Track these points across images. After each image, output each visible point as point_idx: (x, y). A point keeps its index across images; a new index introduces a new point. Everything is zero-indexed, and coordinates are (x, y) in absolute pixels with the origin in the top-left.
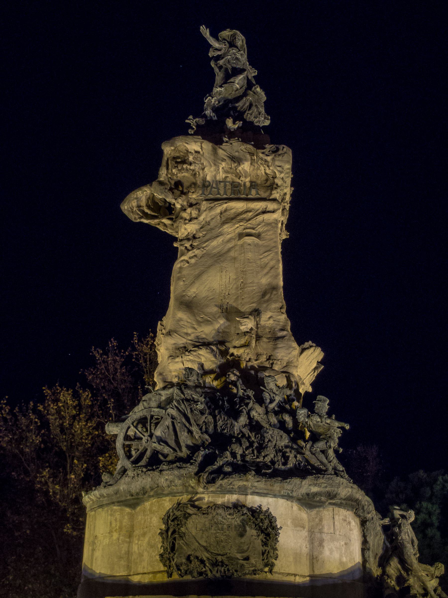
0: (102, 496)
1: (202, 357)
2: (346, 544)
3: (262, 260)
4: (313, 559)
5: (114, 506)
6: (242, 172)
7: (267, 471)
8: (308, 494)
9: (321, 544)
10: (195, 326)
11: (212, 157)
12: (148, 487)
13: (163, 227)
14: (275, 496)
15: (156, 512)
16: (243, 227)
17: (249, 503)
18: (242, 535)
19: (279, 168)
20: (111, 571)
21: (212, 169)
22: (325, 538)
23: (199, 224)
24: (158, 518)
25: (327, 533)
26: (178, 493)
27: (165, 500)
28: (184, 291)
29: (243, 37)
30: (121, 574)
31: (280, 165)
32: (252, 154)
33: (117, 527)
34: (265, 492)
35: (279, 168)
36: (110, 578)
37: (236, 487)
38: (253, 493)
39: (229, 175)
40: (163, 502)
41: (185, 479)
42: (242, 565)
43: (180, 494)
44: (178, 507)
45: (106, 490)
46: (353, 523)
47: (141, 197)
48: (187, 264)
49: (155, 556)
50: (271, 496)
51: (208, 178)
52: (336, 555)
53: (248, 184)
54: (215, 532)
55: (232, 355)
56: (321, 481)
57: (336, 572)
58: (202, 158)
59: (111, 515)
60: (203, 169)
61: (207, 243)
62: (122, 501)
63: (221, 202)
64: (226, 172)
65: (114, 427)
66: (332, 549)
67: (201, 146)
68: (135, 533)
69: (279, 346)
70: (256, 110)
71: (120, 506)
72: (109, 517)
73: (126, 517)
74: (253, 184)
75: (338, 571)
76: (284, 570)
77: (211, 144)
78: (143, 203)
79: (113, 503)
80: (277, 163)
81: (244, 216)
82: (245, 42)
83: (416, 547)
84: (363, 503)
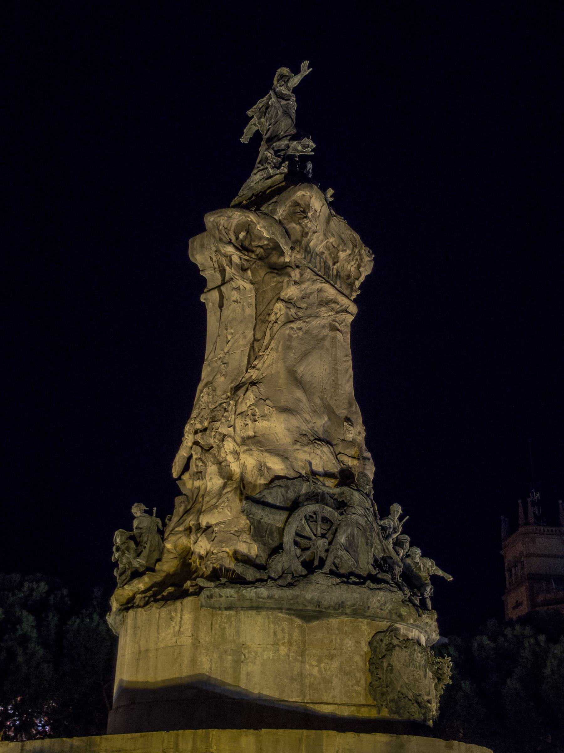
0: (270, 597)
5: (281, 612)
11: (325, 225)
12: (349, 603)
13: (228, 262)
15: (351, 633)
20: (280, 694)
23: (301, 291)
24: (353, 641)
26: (380, 618)
27: (362, 622)
28: (294, 365)
30: (294, 700)
32: (355, 246)
33: (286, 641)
36: (284, 703)
39: (326, 252)
40: (360, 624)
43: (380, 620)
45: (280, 592)
49: (352, 686)
51: (311, 244)
59: (274, 623)
60: (314, 232)
62: (295, 610)
64: (327, 248)
71: (289, 614)
72: (272, 625)
79: (280, 609)
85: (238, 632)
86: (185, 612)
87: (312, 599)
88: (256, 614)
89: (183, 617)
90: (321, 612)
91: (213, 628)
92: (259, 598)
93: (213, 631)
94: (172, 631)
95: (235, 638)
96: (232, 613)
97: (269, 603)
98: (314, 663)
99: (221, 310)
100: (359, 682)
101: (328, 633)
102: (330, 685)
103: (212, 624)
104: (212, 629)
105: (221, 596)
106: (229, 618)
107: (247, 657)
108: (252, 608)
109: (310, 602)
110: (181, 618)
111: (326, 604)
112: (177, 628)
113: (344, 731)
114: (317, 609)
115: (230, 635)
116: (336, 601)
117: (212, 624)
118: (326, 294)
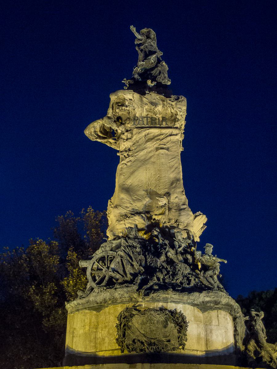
1: (136, 221)
2: (225, 332)
3: (170, 163)
4: (207, 342)
5: (86, 310)
6: (157, 111)
7: (179, 288)
8: (203, 302)
9: (211, 332)
10: (132, 203)
11: (140, 103)
12: (108, 298)
14: (184, 303)
16: (158, 144)
17: (169, 307)
18: (165, 327)
19: (179, 109)
20: (85, 349)
21: (140, 109)
22: (213, 328)
25: (214, 325)
26: (126, 302)
29: (155, 33)
30: (91, 351)
31: (180, 107)
32: (163, 101)
34: (178, 301)
35: (179, 109)
36: (85, 354)
37: (162, 298)
38: (172, 302)
40: (117, 307)
41: (131, 293)
42: (166, 345)
43: (127, 303)
44: (127, 310)
45: (81, 301)
46: (229, 319)
47: (96, 126)
48: (126, 166)
49: (113, 340)
50: (182, 303)
51: (137, 115)
52: (220, 338)
53: (161, 119)
54: (149, 325)
55: (154, 219)
56: (211, 294)
57: (220, 349)
58: (134, 103)
60: (134, 110)
61: (137, 154)
62: (91, 307)
63: (145, 129)
64: (147, 111)
65: (84, 263)
66: (217, 335)
67: (133, 96)
68: (99, 326)
69: (182, 214)
70: (163, 76)
72: (83, 317)
73: (94, 317)
74: (164, 118)
75: (222, 348)
76: (191, 348)
77: (139, 95)
78: (98, 130)
79: (86, 308)
80: (178, 106)
81: (159, 137)
82: (155, 36)
83: (265, 333)
84: (235, 307)
88: (78, 313)
97: (80, 307)
113: (71, 366)
118: (152, 135)
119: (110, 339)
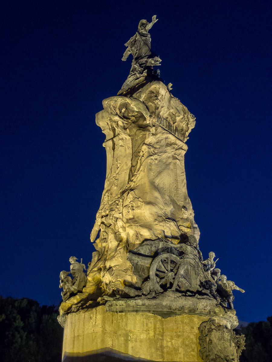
0: (143, 305)
1: (172, 227)
13: (116, 125)
20: (150, 357)
23: (156, 139)
24: (190, 327)
26: (204, 314)
27: (194, 317)
28: (154, 179)
30: (158, 360)
39: (169, 117)
40: (193, 318)
41: (212, 307)
43: (205, 315)
45: (149, 302)
47: (118, 102)
49: (190, 352)
51: (161, 114)
60: (162, 107)
62: (157, 311)
65: (136, 258)
72: (145, 320)
79: (150, 311)
85: (126, 324)
86: (98, 314)
87: (166, 305)
88: (136, 314)
89: (97, 317)
90: (172, 312)
91: (113, 323)
92: (137, 305)
93: (113, 324)
94: (91, 325)
95: (125, 328)
96: (123, 314)
97: (143, 308)
98: (169, 340)
99: (114, 151)
100: (194, 350)
101: (176, 323)
102: (178, 351)
103: (112, 321)
104: (112, 323)
105: (117, 305)
106: (121, 316)
107: (132, 338)
108: (133, 311)
109: (165, 306)
110: (96, 317)
111: (174, 308)
112: (94, 323)
114: (169, 310)
115: (122, 326)
116: (179, 306)
117: (112, 321)
118: (170, 140)
119: (186, 350)
